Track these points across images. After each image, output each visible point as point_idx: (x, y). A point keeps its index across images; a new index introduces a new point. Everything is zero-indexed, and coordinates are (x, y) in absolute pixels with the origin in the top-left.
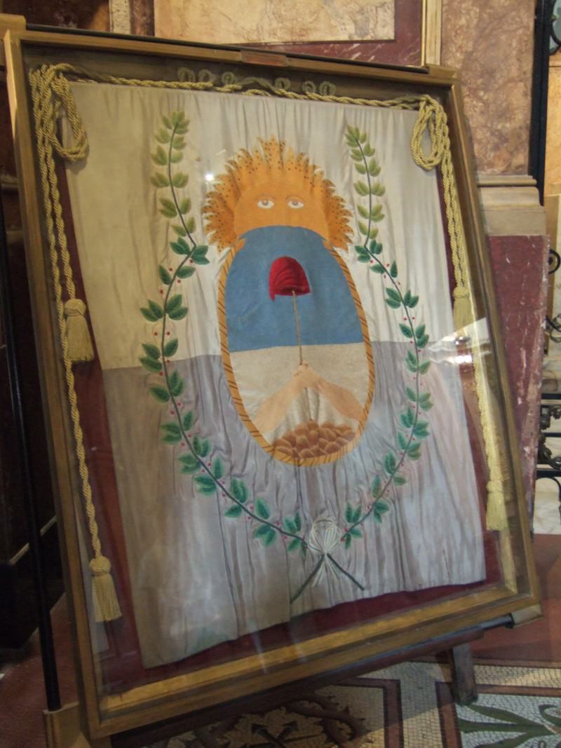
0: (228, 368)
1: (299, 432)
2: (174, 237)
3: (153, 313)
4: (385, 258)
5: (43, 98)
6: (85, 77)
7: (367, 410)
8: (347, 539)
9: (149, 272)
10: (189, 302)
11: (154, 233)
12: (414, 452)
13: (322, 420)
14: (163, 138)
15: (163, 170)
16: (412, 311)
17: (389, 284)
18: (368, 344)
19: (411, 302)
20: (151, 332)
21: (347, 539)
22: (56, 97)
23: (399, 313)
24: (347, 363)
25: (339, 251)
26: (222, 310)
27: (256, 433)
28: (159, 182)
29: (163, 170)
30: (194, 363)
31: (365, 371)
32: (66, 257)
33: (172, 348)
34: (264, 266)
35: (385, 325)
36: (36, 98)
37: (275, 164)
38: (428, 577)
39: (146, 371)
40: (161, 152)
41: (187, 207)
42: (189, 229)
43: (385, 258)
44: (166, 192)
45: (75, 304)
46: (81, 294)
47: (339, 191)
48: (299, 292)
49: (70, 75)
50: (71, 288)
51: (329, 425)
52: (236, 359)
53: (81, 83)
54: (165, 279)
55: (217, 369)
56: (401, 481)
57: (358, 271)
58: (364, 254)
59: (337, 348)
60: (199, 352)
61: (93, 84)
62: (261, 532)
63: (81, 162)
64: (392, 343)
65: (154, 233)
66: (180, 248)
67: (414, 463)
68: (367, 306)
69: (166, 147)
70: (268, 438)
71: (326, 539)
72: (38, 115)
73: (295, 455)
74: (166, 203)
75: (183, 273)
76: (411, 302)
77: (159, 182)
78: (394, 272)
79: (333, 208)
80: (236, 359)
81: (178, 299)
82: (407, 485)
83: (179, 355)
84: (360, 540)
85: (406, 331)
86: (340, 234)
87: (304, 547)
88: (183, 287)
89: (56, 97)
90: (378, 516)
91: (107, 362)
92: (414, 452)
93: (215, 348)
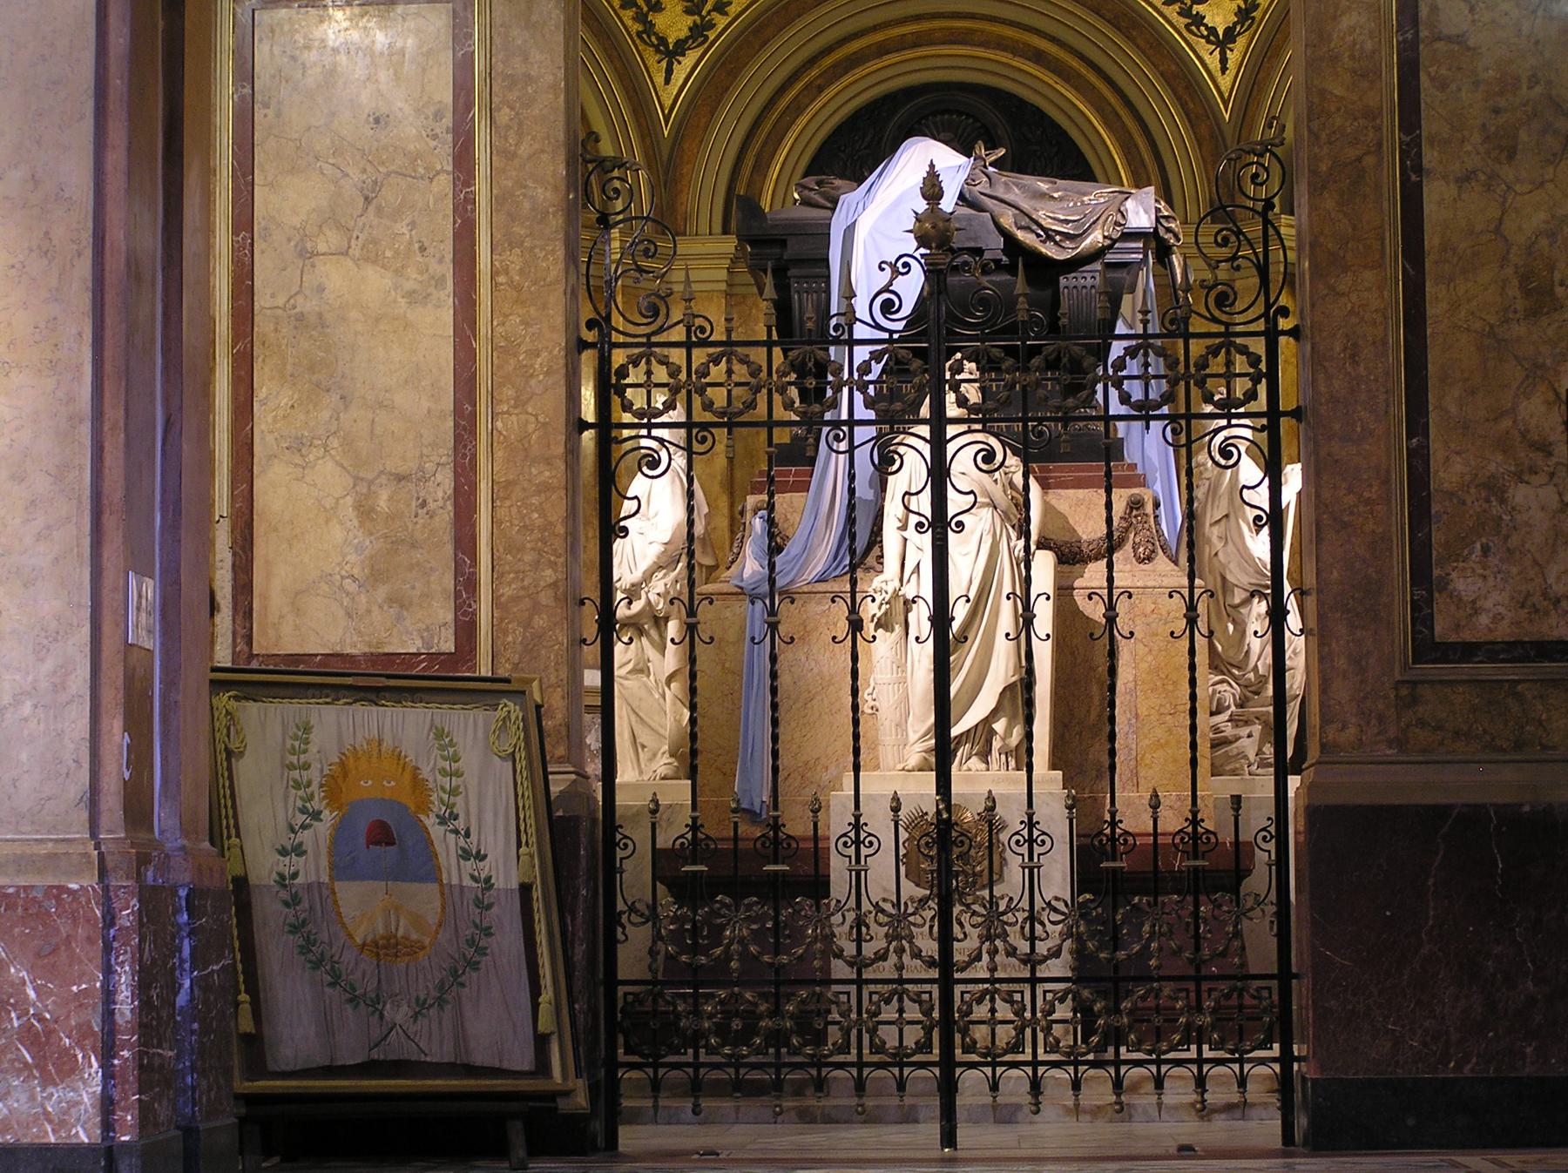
0: (334, 893)
1: (383, 938)
2: (299, 803)
3: (283, 852)
4: (460, 824)
5: (220, 714)
6: (247, 699)
7: (437, 932)
8: (415, 1016)
9: (282, 826)
10: (309, 847)
11: (286, 798)
12: (475, 966)
13: (400, 933)
14: (296, 738)
15: (294, 759)
16: (481, 864)
17: (462, 842)
18: (441, 884)
19: (480, 857)
20: (285, 865)
21: (415, 1016)
22: (228, 713)
23: (469, 865)
24: (425, 900)
25: (422, 817)
26: (330, 854)
27: (350, 936)
28: (291, 767)
29: (294, 759)
30: (309, 886)
31: (438, 903)
32: (230, 812)
33: (295, 875)
34: (363, 826)
35: (455, 871)
36: (216, 714)
37: (375, 754)
38: (480, 1058)
39: (277, 888)
40: (293, 747)
41: (309, 784)
42: (310, 798)
43: (460, 824)
44: (295, 774)
45: (234, 840)
46: (238, 835)
47: (425, 773)
48: (388, 844)
49: (237, 698)
50: (233, 832)
51: (405, 938)
52: (338, 885)
53: (244, 703)
54: (293, 831)
55: (326, 893)
56: (462, 985)
57: (436, 831)
58: (443, 821)
59: (415, 886)
60: (313, 878)
61: (251, 703)
62: (351, 1001)
63: (242, 754)
64: (462, 887)
65: (286, 798)
66: (303, 811)
67: (474, 975)
68: (442, 860)
69: (297, 744)
70: (359, 940)
71: (399, 1014)
72: (217, 724)
73: (378, 955)
74: (295, 781)
75: (304, 827)
76: (480, 857)
77: (291, 767)
78: (467, 835)
79: (417, 783)
80: (338, 885)
81: (301, 844)
82: (467, 990)
83: (299, 880)
84: (426, 1022)
85: (475, 879)
86: (424, 807)
87: (382, 1016)
88: (305, 836)
89: (228, 713)
90: (441, 1007)
91: (253, 880)
92: (475, 966)
93: (325, 879)
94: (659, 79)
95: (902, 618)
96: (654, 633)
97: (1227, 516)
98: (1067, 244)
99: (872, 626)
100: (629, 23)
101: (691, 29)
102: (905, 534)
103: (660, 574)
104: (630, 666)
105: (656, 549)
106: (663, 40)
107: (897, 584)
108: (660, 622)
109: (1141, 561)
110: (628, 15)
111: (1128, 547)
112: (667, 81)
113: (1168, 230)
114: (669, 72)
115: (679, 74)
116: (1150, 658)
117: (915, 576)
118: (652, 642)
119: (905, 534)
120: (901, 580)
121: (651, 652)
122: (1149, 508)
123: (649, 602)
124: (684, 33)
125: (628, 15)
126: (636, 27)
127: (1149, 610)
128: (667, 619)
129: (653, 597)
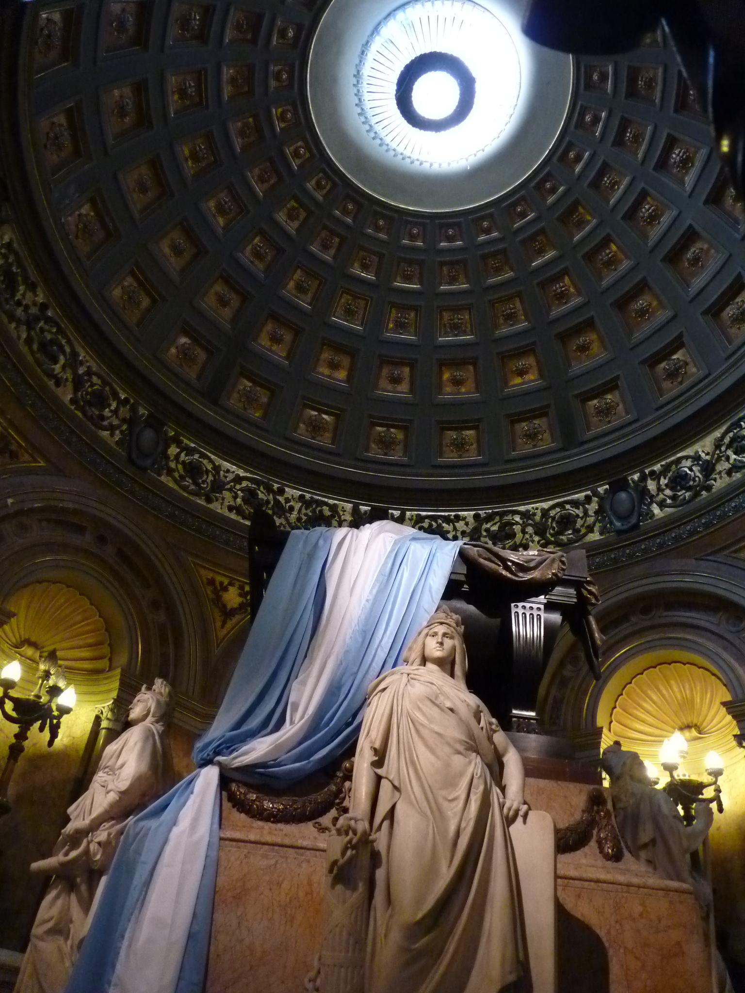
94: (219, 624)
95: (365, 874)
96: (83, 888)
97: (653, 841)
98: (521, 574)
99: (330, 879)
100: (209, 593)
101: (240, 605)
102: (379, 771)
103: (107, 825)
104: (50, 925)
105: (112, 797)
106: (224, 606)
107: (367, 825)
108: (93, 875)
109: (608, 857)
110: (209, 590)
111: (593, 843)
112: (223, 627)
113: (590, 592)
114: (224, 623)
115: (229, 625)
116: (644, 976)
117: (386, 824)
118: (80, 901)
119: (379, 771)
120: (371, 822)
121: (76, 911)
122: (610, 806)
123: (87, 852)
124: (236, 606)
125: (209, 590)
126: (211, 596)
127: (637, 909)
128: (101, 873)
129: (93, 847)
